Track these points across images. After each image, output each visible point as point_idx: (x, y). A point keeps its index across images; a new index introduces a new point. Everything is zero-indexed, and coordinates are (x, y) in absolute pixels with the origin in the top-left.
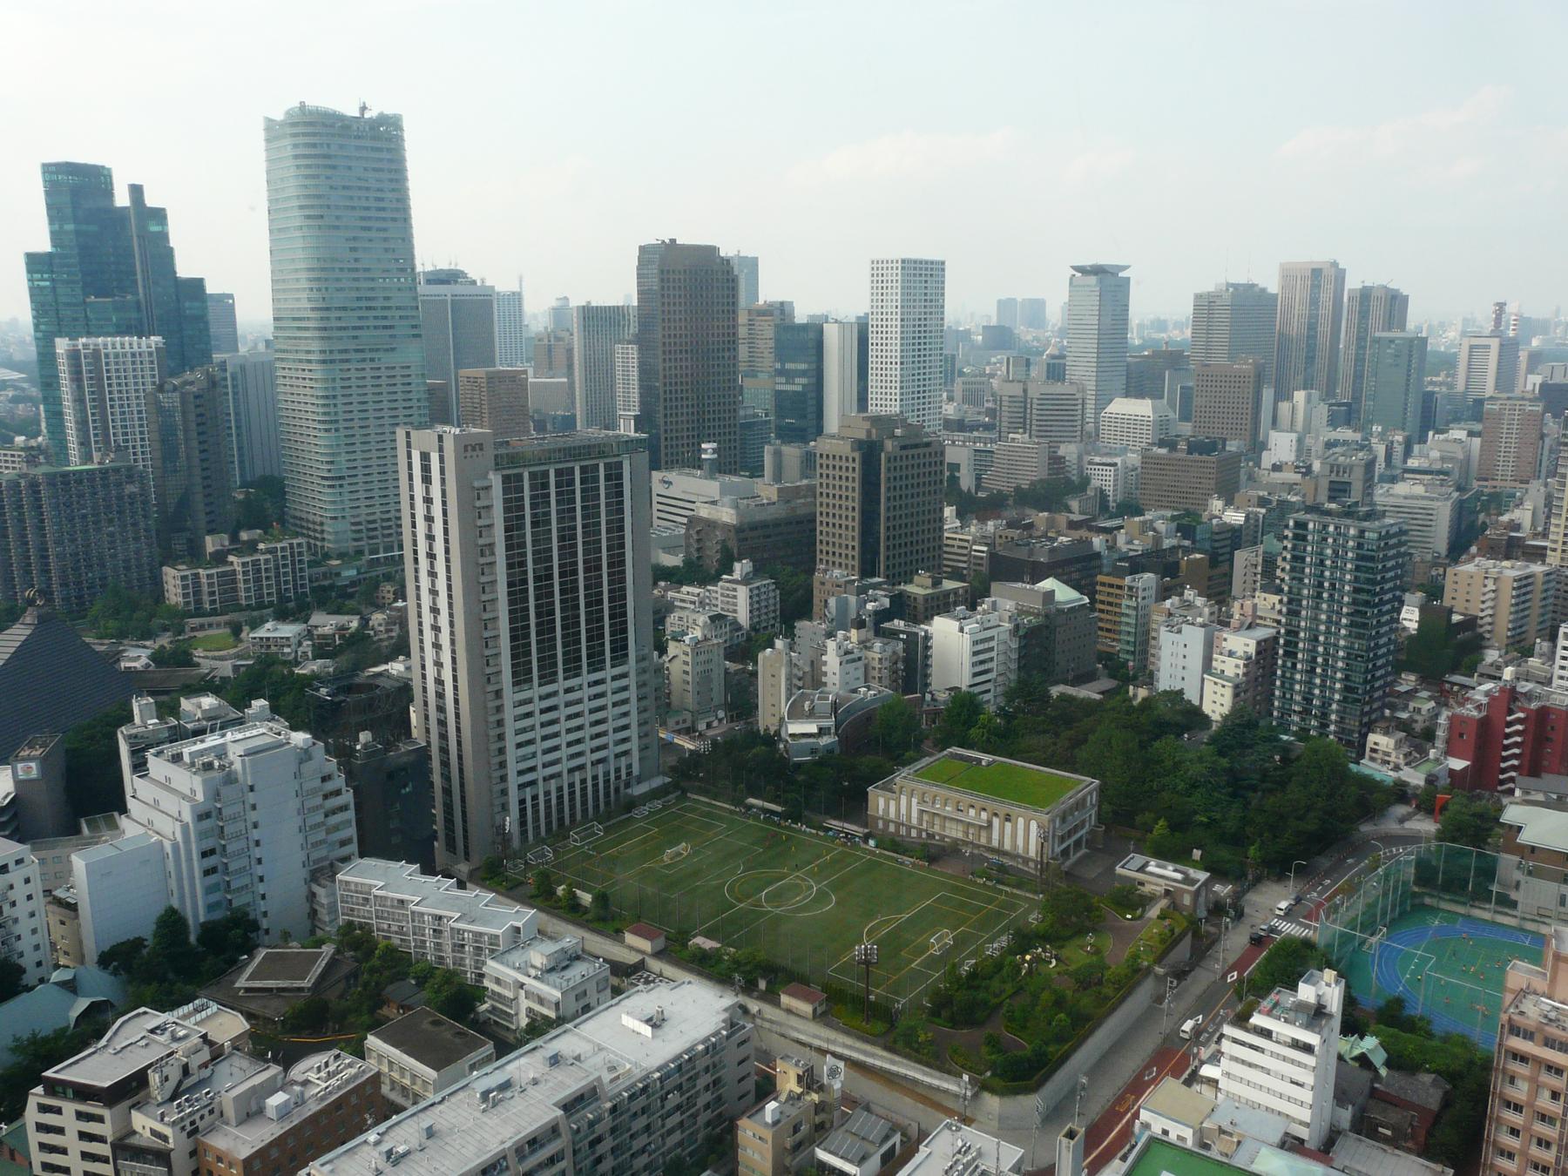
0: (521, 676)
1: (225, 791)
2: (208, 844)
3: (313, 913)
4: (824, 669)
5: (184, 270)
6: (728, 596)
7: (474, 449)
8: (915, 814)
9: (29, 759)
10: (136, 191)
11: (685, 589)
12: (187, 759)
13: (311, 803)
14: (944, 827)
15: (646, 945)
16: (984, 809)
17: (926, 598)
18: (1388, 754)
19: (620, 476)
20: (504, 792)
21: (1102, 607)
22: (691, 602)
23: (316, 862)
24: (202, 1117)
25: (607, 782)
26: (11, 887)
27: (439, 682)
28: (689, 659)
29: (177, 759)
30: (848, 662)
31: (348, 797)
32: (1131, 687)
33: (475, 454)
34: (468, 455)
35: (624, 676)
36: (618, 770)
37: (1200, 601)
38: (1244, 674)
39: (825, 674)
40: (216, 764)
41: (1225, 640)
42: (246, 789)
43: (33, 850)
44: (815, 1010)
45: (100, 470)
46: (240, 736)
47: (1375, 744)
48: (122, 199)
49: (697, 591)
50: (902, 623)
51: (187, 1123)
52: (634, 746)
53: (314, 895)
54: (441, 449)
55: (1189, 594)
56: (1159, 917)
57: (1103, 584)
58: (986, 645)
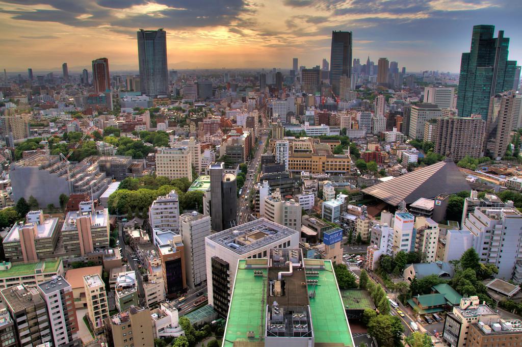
1: (497, 226)
2: (487, 240)
3: (514, 274)
5: (510, 58)
9: (439, 200)
10: (501, 33)
12: (487, 213)
23: (519, 258)
24: (473, 319)
26: (431, 233)
29: (484, 212)
40: (496, 217)
42: (504, 228)
43: (439, 226)
45: (472, 120)
46: (505, 211)
48: (496, 35)
51: (469, 318)
53: (516, 268)
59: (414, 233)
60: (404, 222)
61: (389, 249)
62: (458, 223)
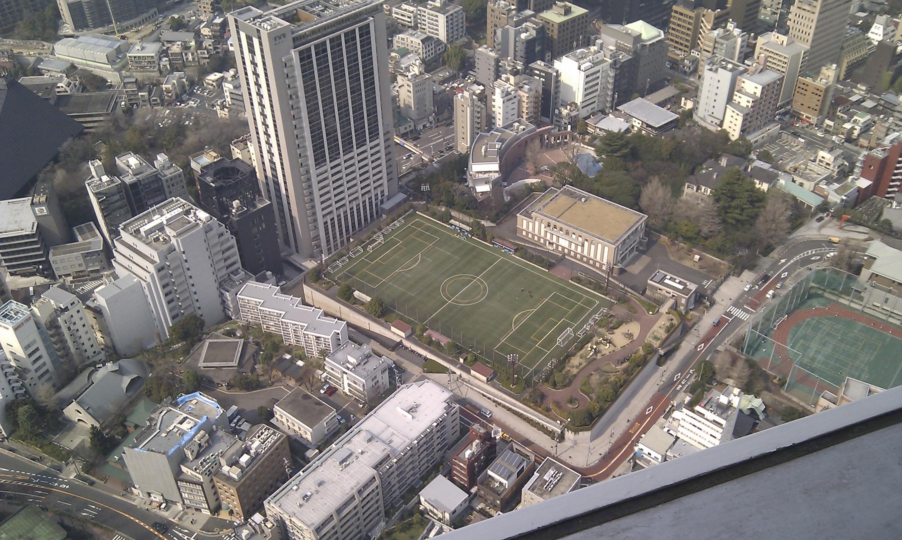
0: (319, 160)
4: (493, 103)
6: (432, 19)
7: (280, 38)
8: (543, 230)
11: (404, 6)
13: (216, 258)
14: (558, 241)
15: (403, 334)
16: (580, 236)
17: (562, 25)
18: (828, 164)
19: (368, 33)
20: (315, 220)
21: (673, 32)
22: (409, 17)
23: (220, 278)
25: (371, 203)
26: (72, 316)
27: (272, 162)
28: (411, 89)
30: (508, 100)
31: (233, 241)
32: (683, 99)
33: (281, 41)
34: (277, 42)
35: (377, 145)
36: (376, 195)
37: (737, 32)
38: (752, 107)
39: (494, 112)
41: (744, 82)
44: (487, 379)
47: (823, 157)
49: (412, 9)
50: (543, 64)
52: (385, 181)
54: (259, 38)
55: (730, 26)
56: (666, 313)
57: (676, 12)
58: (594, 76)
59: (41, 333)
60: (15, 329)
61: (14, 385)
62: (92, 223)
